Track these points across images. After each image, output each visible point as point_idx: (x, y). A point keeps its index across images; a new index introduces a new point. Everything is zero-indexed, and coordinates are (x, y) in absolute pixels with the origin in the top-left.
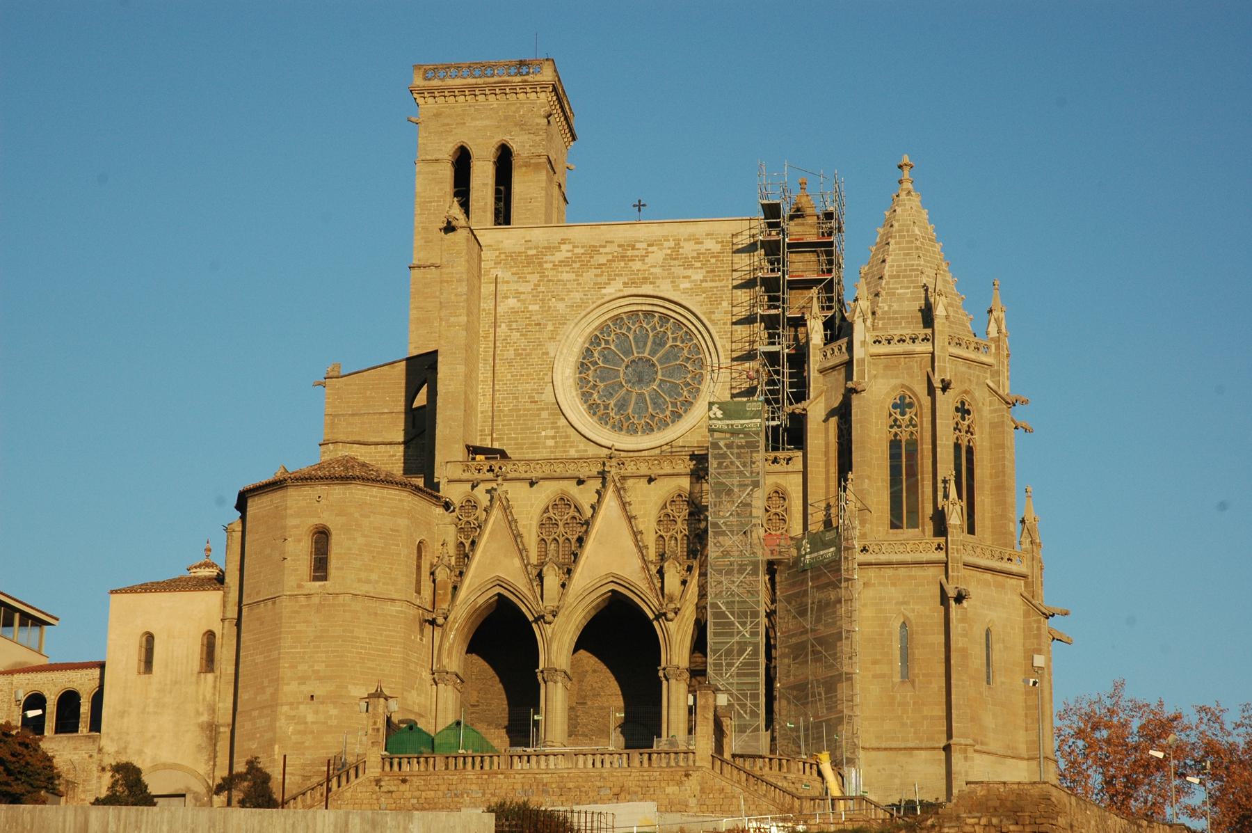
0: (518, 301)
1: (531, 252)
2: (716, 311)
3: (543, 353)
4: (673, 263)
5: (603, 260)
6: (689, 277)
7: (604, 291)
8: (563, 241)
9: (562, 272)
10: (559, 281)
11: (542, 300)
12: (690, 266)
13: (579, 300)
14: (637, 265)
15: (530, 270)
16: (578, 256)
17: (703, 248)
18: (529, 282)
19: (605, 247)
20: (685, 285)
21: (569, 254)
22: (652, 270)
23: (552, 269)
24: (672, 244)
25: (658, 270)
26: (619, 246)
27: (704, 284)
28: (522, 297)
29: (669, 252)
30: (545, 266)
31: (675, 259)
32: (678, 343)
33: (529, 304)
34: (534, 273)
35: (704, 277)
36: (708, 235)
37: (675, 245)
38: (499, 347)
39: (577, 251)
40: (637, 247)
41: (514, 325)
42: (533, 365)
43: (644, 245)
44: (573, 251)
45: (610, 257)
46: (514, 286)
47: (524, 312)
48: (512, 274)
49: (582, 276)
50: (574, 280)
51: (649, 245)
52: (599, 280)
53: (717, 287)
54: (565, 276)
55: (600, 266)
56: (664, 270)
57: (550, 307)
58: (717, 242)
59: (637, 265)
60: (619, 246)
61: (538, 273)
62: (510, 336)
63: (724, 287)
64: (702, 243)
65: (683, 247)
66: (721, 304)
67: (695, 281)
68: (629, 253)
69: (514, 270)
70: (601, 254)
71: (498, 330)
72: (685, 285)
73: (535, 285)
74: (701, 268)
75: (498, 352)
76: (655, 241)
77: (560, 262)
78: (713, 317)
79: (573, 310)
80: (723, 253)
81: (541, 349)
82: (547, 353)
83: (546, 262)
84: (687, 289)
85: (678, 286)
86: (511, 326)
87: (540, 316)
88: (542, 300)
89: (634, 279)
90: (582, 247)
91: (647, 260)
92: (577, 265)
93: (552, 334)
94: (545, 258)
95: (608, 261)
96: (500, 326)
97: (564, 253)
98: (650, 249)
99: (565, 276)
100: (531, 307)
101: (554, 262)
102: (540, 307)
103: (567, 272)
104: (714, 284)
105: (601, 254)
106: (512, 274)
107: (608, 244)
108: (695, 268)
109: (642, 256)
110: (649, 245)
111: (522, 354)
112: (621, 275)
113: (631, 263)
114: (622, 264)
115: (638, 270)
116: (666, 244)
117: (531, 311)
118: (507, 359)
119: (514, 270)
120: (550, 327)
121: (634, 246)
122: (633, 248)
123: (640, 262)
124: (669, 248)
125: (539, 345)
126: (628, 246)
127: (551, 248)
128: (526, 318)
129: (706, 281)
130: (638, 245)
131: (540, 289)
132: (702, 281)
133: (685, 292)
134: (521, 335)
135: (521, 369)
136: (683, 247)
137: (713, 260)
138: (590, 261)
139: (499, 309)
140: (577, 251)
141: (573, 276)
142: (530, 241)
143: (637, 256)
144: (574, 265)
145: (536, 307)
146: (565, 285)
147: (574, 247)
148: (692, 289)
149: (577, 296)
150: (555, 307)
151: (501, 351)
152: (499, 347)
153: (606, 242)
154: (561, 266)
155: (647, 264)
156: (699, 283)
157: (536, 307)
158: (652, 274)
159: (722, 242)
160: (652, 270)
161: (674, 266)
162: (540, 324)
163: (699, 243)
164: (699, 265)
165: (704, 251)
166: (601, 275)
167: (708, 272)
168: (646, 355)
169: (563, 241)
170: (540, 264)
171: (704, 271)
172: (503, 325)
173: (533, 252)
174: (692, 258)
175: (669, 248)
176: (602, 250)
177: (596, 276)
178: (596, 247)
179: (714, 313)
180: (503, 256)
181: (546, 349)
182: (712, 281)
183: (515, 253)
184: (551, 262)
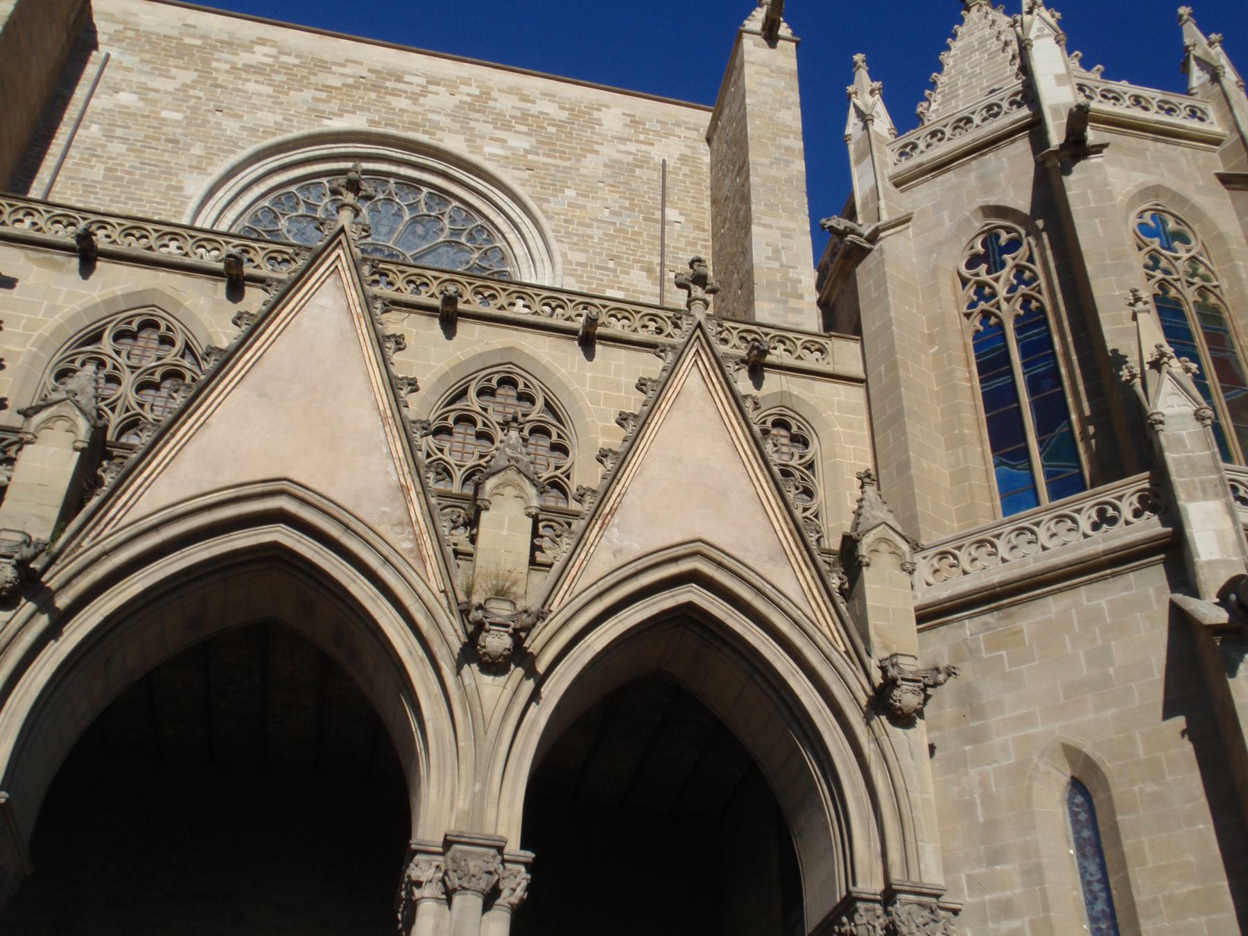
0: (141, 99)
1: (187, 40)
2: (552, 199)
3: (170, 187)
4: (473, 115)
5: (337, 82)
6: (504, 141)
7: (326, 122)
8: (263, 42)
9: (248, 80)
10: (239, 90)
11: (194, 109)
12: (507, 127)
13: (271, 124)
14: (403, 103)
15: (181, 63)
16: (285, 66)
17: (534, 109)
18: (174, 78)
19: (343, 66)
20: (496, 150)
21: (270, 61)
22: (430, 116)
23: (226, 72)
24: (476, 92)
25: (443, 120)
26: (370, 71)
27: (530, 157)
28: (152, 95)
29: (468, 99)
30: (214, 64)
31: (478, 111)
32: (463, 240)
33: (164, 109)
34: (187, 69)
35: (532, 146)
36: (545, 95)
37: (482, 93)
38: (72, 157)
39: (284, 59)
40: (405, 80)
41: (119, 132)
42: (141, 200)
43: (423, 81)
44: (277, 58)
45: (350, 81)
46: (136, 78)
47: (147, 117)
48: (142, 61)
49: (287, 94)
50: (268, 96)
51: (428, 82)
52: (321, 106)
53: (558, 166)
54: (251, 87)
55: (327, 88)
56: (454, 121)
57: (206, 122)
58: (562, 108)
59: (403, 103)
60: (370, 71)
61: (196, 70)
62: (104, 146)
63: (571, 168)
64: (533, 102)
65: (496, 100)
66: (563, 191)
67: (510, 148)
68: (390, 84)
69: (148, 56)
70: (334, 73)
71: (80, 131)
72: (496, 150)
73: (184, 85)
74: (531, 135)
75: (68, 163)
76: (443, 79)
77: (245, 65)
78: (545, 206)
79: (254, 136)
80: (574, 124)
81: (166, 180)
82: (180, 189)
83: (218, 60)
84: (499, 156)
85: (481, 148)
86: (113, 131)
87: (180, 130)
88: (194, 109)
89: (394, 120)
90: (297, 56)
91: (422, 100)
92: (277, 78)
93: (200, 162)
94: (217, 55)
95: (344, 85)
96: (87, 127)
97: (260, 55)
98: (431, 88)
99: (251, 87)
100: (164, 114)
101: (236, 63)
102: (185, 118)
103: (257, 82)
104: (550, 161)
105: (334, 73)
106: (142, 61)
107: (349, 64)
108: (516, 132)
109: (413, 93)
110: (428, 82)
111: (121, 179)
112: (368, 110)
113: (389, 98)
114: (373, 95)
115: (402, 110)
116: (463, 88)
117: (164, 120)
118: (85, 179)
119: (148, 56)
120: (198, 150)
121: (403, 77)
122: (399, 79)
123: (409, 102)
124: (469, 95)
125: (161, 172)
126: (390, 74)
127: (230, 44)
128: (149, 127)
129: (536, 154)
130: (407, 78)
131: (191, 92)
132: (527, 152)
133: (492, 157)
134: (128, 150)
135: (111, 201)
136: (496, 100)
137: (553, 130)
138: (308, 78)
139: (93, 102)
140: (284, 59)
141: (270, 90)
142: (195, 27)
143: (406, 92)
144: (274, 76)
145: (179, 116)
146: (250, 98)
147: (281, 52)
148: (506, 158)
149: (269, 118)
150: (220, 124)
151: (75, 164)
152: (72, 157)
153: (347, 61)
154: (247, 72)
155: (422, 105)
156: (521, 152)
157: (179, 116)
158: (429, 120)
159: (572, 109)
160: (430, 116)
161: (478, 120)
162: (176, 142)
163: (525, 99)
164: (525, 129)
165: (536, 114)
166: (327, 101)
167: (539, 142)
168: (390, 244)
169: (263, 42)
170: (206, 62)
171: (533, 140)
172: (95, 128)
173: (198, 42)
174: (512, 117)
175: (469, 95)
176: (334, 68)
177: (316, 99)
178: (326, 62)
179: (547, 201)
180: (130, 33)
181: (181, 182)
182: (549, 156)
183: (157, 34)
184: (227, 62)
